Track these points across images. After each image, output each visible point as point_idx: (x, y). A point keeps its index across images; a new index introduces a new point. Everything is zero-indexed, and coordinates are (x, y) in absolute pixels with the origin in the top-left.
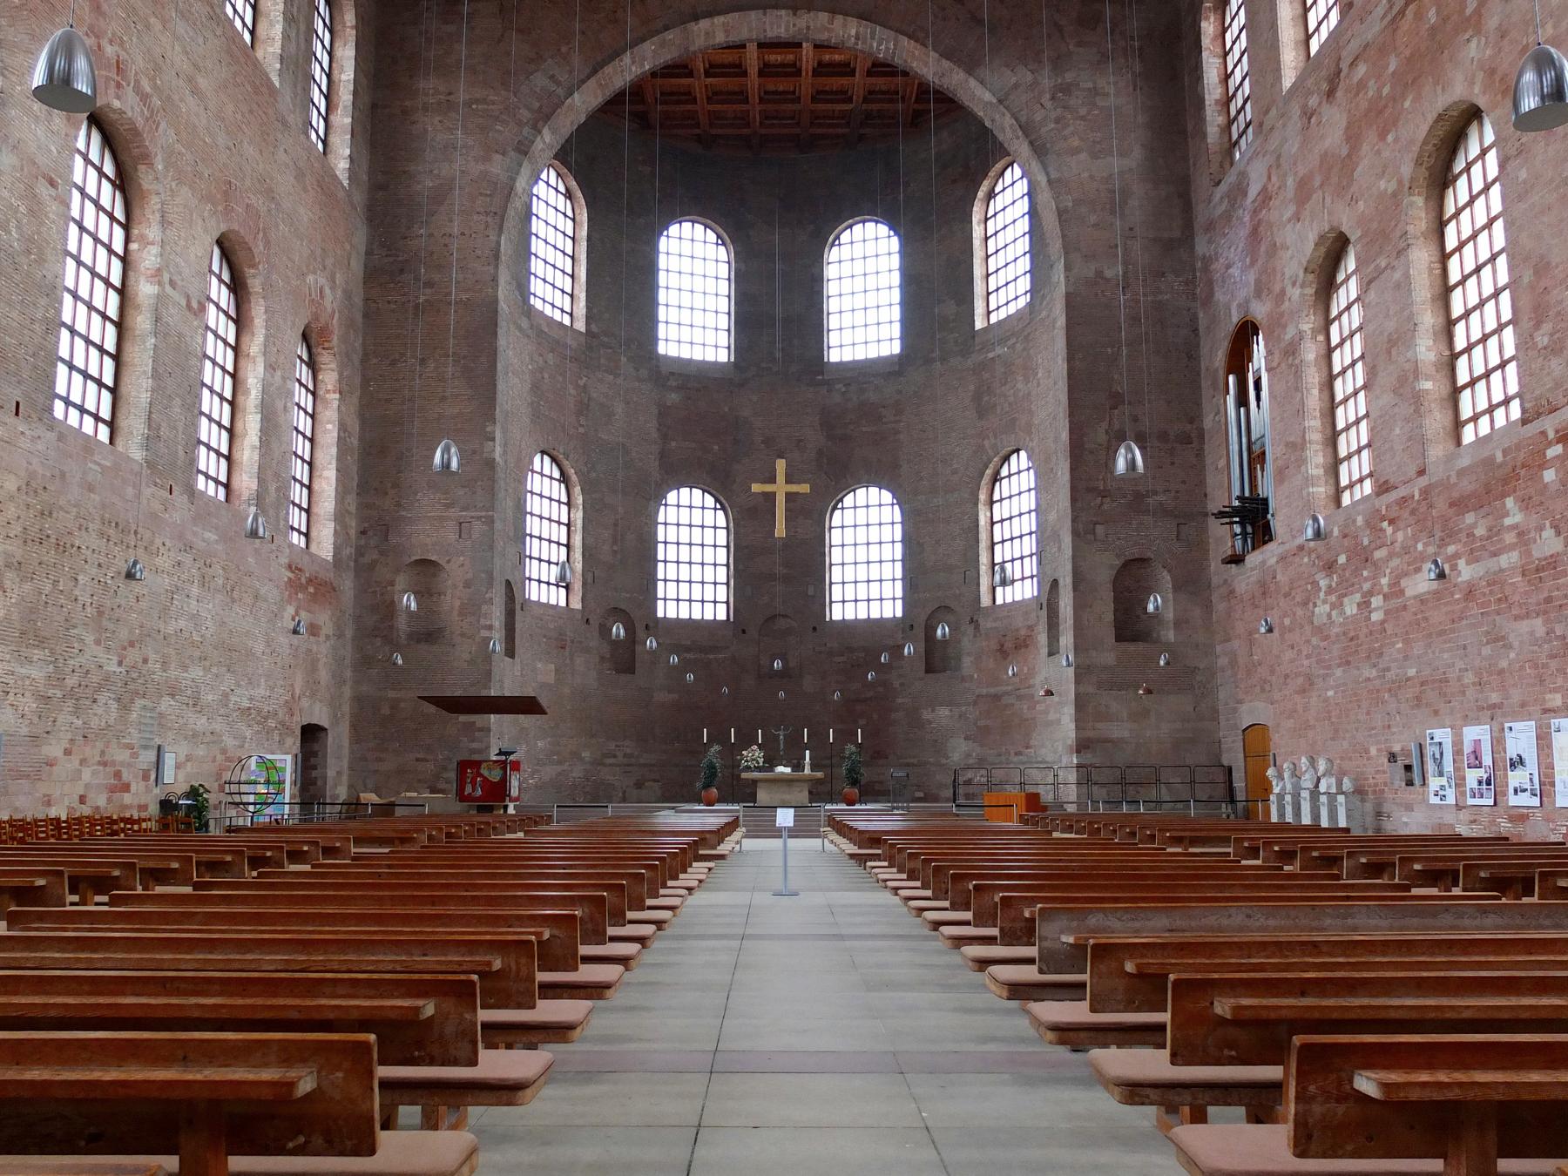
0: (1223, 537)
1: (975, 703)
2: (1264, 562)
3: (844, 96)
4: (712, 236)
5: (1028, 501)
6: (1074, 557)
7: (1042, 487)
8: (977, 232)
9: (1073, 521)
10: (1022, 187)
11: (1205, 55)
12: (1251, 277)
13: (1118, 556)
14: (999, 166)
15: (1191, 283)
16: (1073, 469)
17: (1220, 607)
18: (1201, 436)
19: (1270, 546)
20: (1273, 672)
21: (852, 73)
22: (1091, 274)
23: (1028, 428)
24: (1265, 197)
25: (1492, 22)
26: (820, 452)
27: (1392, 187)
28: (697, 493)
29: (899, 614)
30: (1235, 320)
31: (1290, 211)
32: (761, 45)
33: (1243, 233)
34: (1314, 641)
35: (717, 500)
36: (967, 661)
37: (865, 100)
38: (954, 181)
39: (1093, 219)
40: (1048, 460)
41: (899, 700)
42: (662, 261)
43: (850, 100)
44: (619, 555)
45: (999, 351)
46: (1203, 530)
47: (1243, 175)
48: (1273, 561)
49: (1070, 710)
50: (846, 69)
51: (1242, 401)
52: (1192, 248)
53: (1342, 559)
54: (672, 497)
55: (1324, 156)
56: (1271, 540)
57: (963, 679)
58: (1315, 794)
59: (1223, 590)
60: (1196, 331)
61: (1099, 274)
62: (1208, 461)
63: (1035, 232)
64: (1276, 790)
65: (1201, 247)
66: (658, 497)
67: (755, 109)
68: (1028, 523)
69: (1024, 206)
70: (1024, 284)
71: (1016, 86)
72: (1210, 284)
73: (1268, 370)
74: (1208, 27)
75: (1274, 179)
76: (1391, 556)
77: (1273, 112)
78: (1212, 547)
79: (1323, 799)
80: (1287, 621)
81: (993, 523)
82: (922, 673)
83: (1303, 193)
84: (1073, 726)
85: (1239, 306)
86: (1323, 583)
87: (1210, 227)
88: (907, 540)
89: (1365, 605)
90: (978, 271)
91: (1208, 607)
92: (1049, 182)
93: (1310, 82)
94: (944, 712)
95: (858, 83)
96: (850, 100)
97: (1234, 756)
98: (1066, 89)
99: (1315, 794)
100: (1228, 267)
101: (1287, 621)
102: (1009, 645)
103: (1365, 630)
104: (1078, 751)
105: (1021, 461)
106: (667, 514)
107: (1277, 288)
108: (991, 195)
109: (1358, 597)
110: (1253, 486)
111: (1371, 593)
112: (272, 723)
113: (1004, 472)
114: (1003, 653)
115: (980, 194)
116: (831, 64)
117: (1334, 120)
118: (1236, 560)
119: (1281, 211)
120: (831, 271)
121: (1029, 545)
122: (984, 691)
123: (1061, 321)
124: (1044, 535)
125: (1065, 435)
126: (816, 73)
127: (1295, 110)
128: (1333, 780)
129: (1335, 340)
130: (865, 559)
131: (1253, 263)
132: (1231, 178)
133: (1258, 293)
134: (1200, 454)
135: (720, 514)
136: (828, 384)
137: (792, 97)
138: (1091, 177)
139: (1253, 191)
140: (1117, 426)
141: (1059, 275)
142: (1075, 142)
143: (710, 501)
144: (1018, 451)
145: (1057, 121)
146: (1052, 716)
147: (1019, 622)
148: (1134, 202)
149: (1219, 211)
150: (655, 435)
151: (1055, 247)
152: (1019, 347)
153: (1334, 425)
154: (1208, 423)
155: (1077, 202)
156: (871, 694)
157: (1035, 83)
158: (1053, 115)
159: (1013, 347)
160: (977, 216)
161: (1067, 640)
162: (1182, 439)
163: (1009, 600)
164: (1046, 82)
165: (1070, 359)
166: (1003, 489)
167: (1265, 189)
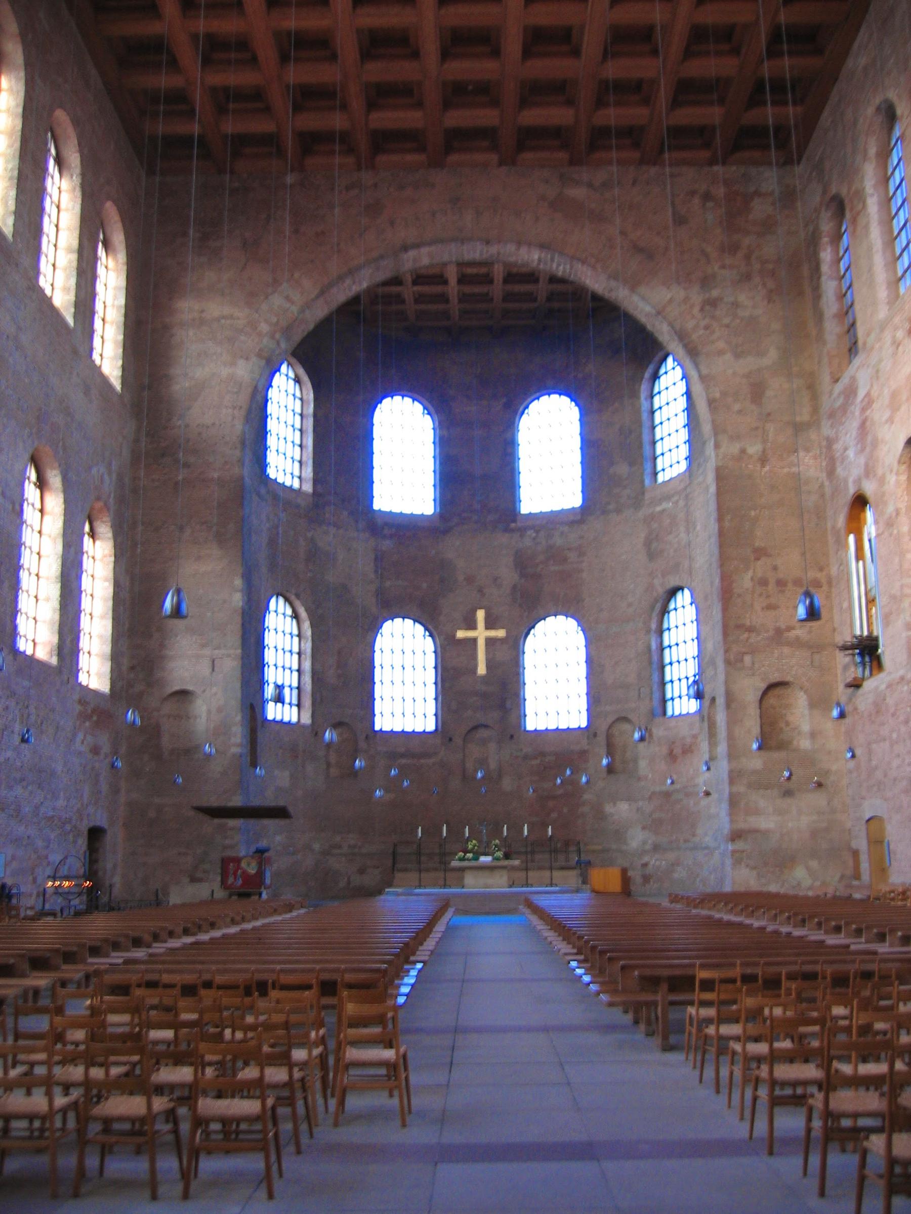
1: (650, 798)
2: (877, 688)
3: (531, 297)
4: (418, 407)
5: (691, 631)
8: (645, 405)
10: (679, 371)
11: (823, 278)
12: (862, 460)
13: (762, 679)
14: (660, 355)
16: (725, 610)
18: (830, 583)
19: (882, 675)
20: (885, 776)
21: (536, 281)
24: (869, 401)
26: (514, 587)
29: (584, 724)
30: (852, 490)
31: (887, 414)
32: (460, 265)
33: (855, 424)
35: (426, 629)
36: (643, 764)
37: (549, 299)
39: (737, 407)
41: (586, 796)
44: (343, 679)
47: (853, 379)
48: (883, 687)
49: (725, 806)
50: (531, 277)
51: (859, 556)
54: (388, 626)
57: (639, 779)
61: (743, 451)
63: (690, 409)
67: (455, 307)
68: (692, 649)
69: (682, 387)
70: (684, 450)
71: (671, 301)
75: (875, 388)
77: (873, 336)
80: (894, 735)
81: (662, 649)
82: (604, 775)
84: (727, 819)
85: (854, 482)
87: (832, 415)
88: (589, 661)
90: (646, 438)
93: (897, 320)
95: (542, 289)
96: (535, 300)
98: (713, 303)
100: (846, 449)
101: (894, 735)
102: (677, 751)
105: (684, 598)
107: (880, 472)
108: (656, 376)
112: (68, 827)
113: (672, 605)
114: (672, 757)
115: (647, 375)
118: (856, 685)
119: (879, 413)
122: (658, 789)
123: (713, 489)
125: (717, 581)
131: (863, 450)
132: (845, 381)
136: (522, 531)
137: (486, 298)
138: (734, 374)
139: (861, 393)
140: (759, 575)
142: (721, 345)
143: (420, 628)
144: (682, 589)
145: (706, 328)
146: (713, 810)
148: (769, 393)
150: (372, 576)
151: (707, 429)
154: (834, 571)
155: (724, 394)
156: (560, 792)
157: (686, 299)
158: (703, 323)
159: (677, 502)
160: (643, 395)
161: (722, 749)
163: (677, 713)
164: (697, 297)
165: (720, 519)
166: (673, 619)
167: (868, 394)
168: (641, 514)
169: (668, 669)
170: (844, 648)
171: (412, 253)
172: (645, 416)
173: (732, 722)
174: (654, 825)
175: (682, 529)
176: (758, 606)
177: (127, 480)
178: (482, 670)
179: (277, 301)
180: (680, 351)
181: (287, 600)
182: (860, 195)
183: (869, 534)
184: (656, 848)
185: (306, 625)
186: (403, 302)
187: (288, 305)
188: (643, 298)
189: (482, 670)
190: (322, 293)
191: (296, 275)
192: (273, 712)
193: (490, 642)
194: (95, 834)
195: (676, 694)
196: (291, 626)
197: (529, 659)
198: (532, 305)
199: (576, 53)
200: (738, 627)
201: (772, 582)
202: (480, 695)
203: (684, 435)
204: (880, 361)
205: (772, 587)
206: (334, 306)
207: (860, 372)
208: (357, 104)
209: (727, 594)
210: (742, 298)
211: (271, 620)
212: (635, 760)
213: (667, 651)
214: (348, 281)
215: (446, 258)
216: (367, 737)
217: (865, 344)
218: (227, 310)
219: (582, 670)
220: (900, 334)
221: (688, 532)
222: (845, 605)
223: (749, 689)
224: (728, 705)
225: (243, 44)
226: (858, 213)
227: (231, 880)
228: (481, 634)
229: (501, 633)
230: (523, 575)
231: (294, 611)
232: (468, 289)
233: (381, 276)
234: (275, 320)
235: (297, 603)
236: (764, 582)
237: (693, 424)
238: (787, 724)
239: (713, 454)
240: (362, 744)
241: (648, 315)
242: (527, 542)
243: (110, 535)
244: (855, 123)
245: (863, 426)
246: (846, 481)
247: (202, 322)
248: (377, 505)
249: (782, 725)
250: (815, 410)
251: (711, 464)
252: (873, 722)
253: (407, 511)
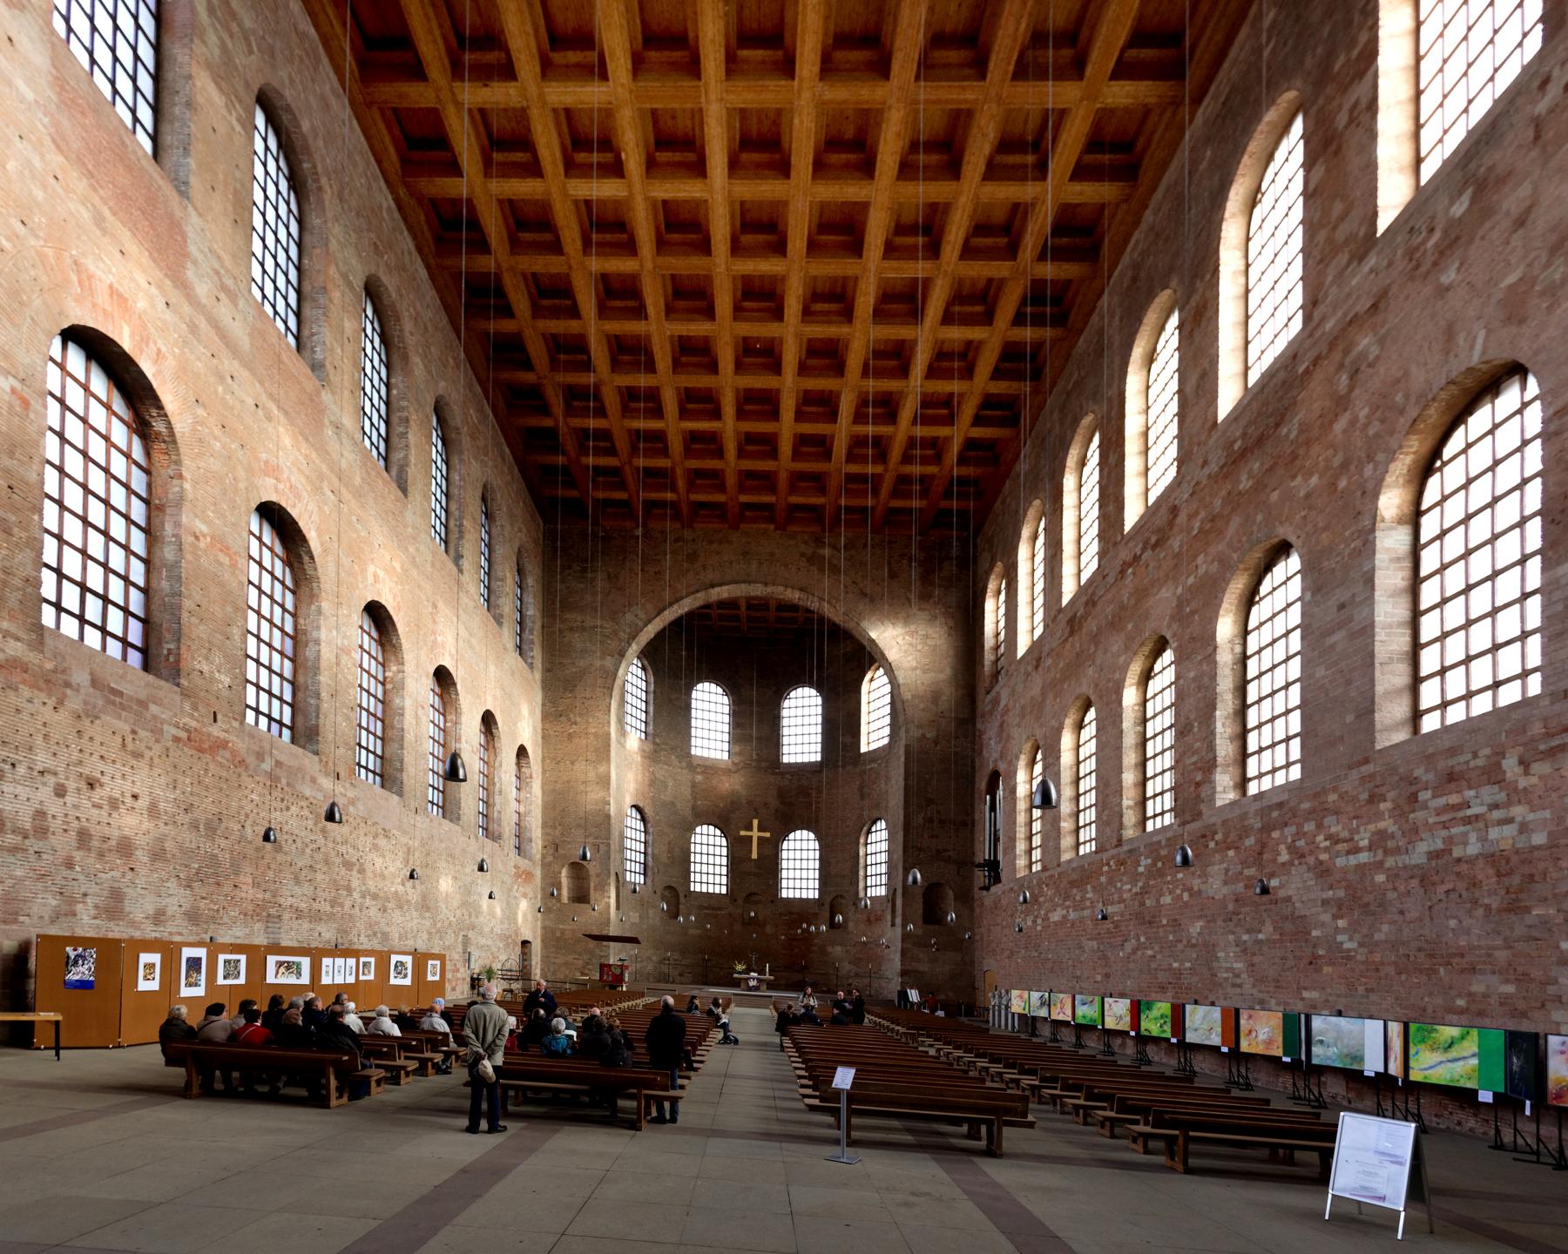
24: (1007, 710)
25: (1098, 662)
65: (979, 726)
66: (691, 830)
87: (983, 716)
94: (839, 949)
119: (1012, 719)
132: (993, 693)
139: (1003, 704)
162: (966, 824)
174: (856, 961)
178: (754, 855)
184: (857, 975)
189: (754, 855)
193: (759, 838)
228: (755, 834)
229: (768, 835)
245: (1001, 725)
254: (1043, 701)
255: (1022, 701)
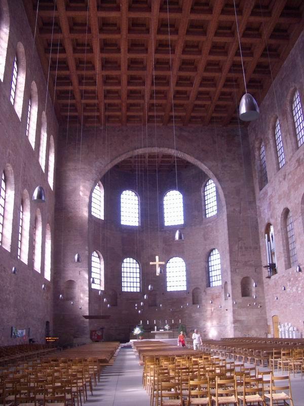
0: (266, 272)
2: (275, 279)
3: (169, 162)
4: (134, 194)
5: (219, 261)
6: (231, 277)
7: (222, 258)
8: (202, 194)
9: (231, 268)
12: (270, 214)
15: (256, 211)
16: (230, 256)
17: (266, 288)
19: (277, 275)
21: (171, 158)
22: (232, 209)
23: (218, 244)
24: (272, 197)
26: (163, 248)
27: (297, 202)
28: (131, 259)
30: (266, 222)
31: (277, 202)
33: (268, 203)
34: (287, 297)
35: (136, 261)
38: (196, 182)
39: (232, 197)
40: (223, 252)
41: (186, 311)
42: (122, 200)
43: (170, 163)
44: (113, 276)
45: (209, 224)
46: (261, 269)
47: (267, 190)
48: (277, 278)
50: (170, 156)
51: (269, 240)
52: (255, 203)
53: (292, 279)
54: (125, 260)
55: (284, 191)
56: (277, 273)
58: (288, 331)
59: (266, 284)
60: (257, 222)
61: (234, 209)
62: (262, 253)
64: (280, 330)
65: (258, 204)
68: (219, 267)
69: (214, 189)
70: (215, 208)
71: (213, 166)
72: (260, 212)
73: (275, 235)
74: (257, 153)
76: (301, 280)
78: (263, 274)
79: (290, 332)
83: (280, 199)
86: (288, 284)
87: (260, 199)
88: (187, 271)
89: (297, 289)
90: (203, 204)
91: (263, 288)
92: (223, 188)
97: (270, 323)
99: (288, 331)
100: (264, 209)
103: (298, 295)
104: (234, 323)
105: (216, 252)
106: (124, 265)
107: (276, 217)
108: (206, 186)
109: (296, 287)
110: (272, 260)
111: (298, 287)
115: (203, 185)
116: (165, 156)
117: (285, 186)
118: (269, 277)
119: (275, 200)
120: (165, 203)
121: (219, 272)
123: (226, 220)
124: (223, 271)
125: (228, 248)
126: (162, 158)
127: (278, 181)
128: (292, 328)
129: (288, 230)
130: (176, 275)
132: (264, 190)
133: (271, 218)
134: (260, 252)
135: (137, 264)
136: (165, 231)
139: (269, 194)
140: (240, 245)
141: (225, 209)
143: (135, 261)
144: (215, 249)
145: (223, 174)
146: (226, 315)
147: (217, 291)
149: (262, 196)
151: (224, 203)
152: (215, 224)
153: (289, 249)
154: (261, 244)
158: (222, 172)
160: (202, 191)
165: (228, 229)
166: (212, 258)
168: (202, 226)
169: (210, 273)
170: (266, 267)
171: (137, 150)
172: (203, 198)
173: (233, 289)
175: (215, 231)
176: (239, 255)
177: (53, 217)
179: (98, 164)
180: (215, 179)
181: (97, 252)
182: (268, 139)
183: (272, 234)
185: (102, 260)
186: (131, 163)
187: (101, 165)
188: (205, 165)
190: (111, 161)
191: (104, 156)
192: (94, 286)
194: (48, 323)
195: (213, 280)
196: (98, 260)
197: (168, 270)
198: (169, 164)
199: (188, 97)
200: (234, 261)
201: (243, 248)
202: (153, 281)
203: (215, 203)
204: (275, 185)
205: (244, 249)
206: (114, 165)
207: (268, 188)
208: (124, 109)
209: (231, 252)
210: (233, 165)
211: (93, 259)
212: (201, 301)
213: (210, 268)
214: (119, 158)
215: (147, 152)
216: (120, 294)
217: (270, 181)
218: (83, 166)
219: (185, 273)
220: (281, 179)
221: (217, 232)
222: (265, 254)
223: (238, 280)
224: (232, 284)
225: (94, 92)
226: (267, 144)
227: (93, 337)
230: (166, 245)
231: (99, 256)
232: (150, 159)
233: (128, 156)
234: (97, 169)
235: (100, 253)
236: (241, 248)
237: (218, 200)
238: (248, 289)
239: (226, 210)
240: (118, 296)
241: (206, 169)
242: (167, 235)
243: (50, 233)
244: (265, 119)
245: (270, 203)
246: (265, 219)
247: (76, 169)
248: (122, 223)
249: (247, 289)
250: (255, 198)
251: (225, 214)
252: (274, 288)
253: (131, 225)
254: (290, 192)
255: (279, 193)
